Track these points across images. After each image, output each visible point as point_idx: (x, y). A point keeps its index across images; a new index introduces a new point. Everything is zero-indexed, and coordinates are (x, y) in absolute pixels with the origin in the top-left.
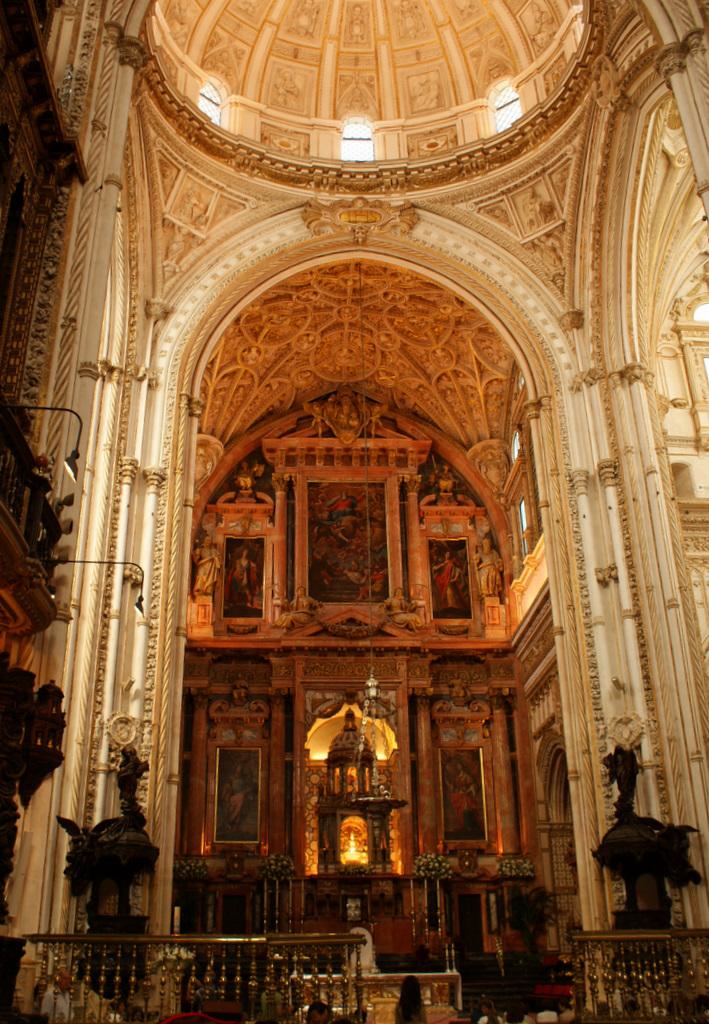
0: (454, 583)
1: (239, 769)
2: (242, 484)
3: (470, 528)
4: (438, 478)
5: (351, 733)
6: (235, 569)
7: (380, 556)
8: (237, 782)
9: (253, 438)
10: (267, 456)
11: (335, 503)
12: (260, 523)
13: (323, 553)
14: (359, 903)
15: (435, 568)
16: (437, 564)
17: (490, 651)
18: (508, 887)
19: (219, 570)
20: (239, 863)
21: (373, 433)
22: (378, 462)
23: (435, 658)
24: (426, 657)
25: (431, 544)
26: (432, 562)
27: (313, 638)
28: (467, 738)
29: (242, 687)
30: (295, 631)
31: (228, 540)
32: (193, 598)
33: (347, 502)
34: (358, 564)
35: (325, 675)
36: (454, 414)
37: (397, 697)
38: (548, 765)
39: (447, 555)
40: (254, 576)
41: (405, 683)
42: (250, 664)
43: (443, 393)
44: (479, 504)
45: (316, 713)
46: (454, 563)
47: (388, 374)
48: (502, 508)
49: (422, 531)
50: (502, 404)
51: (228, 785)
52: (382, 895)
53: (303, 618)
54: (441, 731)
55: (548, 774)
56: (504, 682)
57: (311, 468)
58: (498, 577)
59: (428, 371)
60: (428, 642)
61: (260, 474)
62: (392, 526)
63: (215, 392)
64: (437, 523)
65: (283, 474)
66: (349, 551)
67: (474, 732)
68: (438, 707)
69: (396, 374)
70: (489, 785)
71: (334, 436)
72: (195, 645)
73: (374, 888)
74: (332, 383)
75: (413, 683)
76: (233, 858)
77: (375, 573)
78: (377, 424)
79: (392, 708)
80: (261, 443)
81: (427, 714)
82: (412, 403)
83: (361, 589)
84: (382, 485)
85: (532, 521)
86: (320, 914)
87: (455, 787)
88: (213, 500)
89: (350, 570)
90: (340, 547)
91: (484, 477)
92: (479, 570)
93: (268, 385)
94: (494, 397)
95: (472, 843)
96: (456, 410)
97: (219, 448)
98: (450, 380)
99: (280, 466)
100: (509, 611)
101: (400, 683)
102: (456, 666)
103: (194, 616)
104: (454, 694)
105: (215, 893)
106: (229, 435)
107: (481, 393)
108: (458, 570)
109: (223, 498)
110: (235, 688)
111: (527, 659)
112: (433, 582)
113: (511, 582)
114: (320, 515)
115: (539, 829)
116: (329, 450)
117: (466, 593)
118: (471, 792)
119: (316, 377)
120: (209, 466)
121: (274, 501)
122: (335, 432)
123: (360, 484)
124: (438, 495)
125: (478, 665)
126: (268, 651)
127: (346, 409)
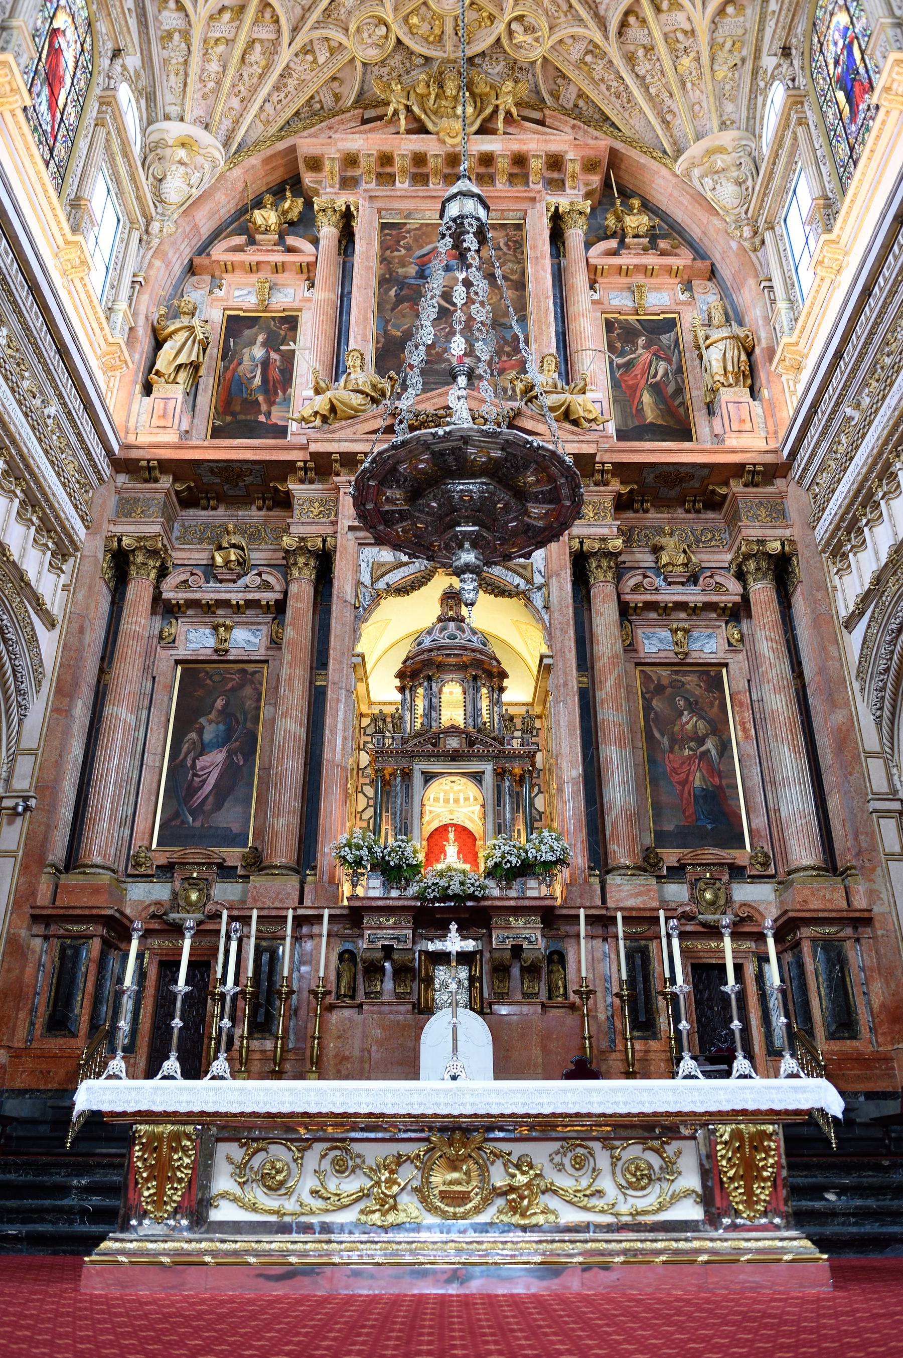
0: (656, 383)
1: (220, 703)
2: (259, 221)
3: (683, 297)
4: (619, 219)
5: (452, 625)
6: (240, 364)
9: (281, 146)
10: (308, 178)
12: (292, 291)
14: (463, 974)
15: (621, 361)
16: (622, 354)
17: (738, 470)
18: (814, 940)
19: (204, 346)
20: (200, 890)
21: (500, 125)
22: (510, 182)
23: (625, 490)
24: (606, 484)
25: (609, 326)
28: (696, 646)
29: (234, 546)
30: (337, 425)
31: (229, 316)
32: (148, 389)
36: (650, 98)
37: (546, 558)
38: (887, 670)
39: (641, 341)
40: (275, 374)
42: (254, 512)
43: (630, 59)
44: (699, 254)
45: (381, 585)
46: (654, 354)
47: (529, 29)
48: (746, 244)
49: (594, 302)
50: (743, 60)
51: (194, 735)
52: (517, 950)
53: (357, 400)
54: (639, 631)
55: (888, 694)
56: (769, 532)
58: (743, 357)
59: (602, 13)
61: (294, 215)
62: (537, 279)
63: (205, 42)
64: (621, 290)
65: (333, 201)
67: (709, 636)
68: (632, 582)
69: (545, 26)
70: (747, 737)
71: (427, 132)
72: (134, 454)
74: (428, 60)
77: (505, 358)
78: (508, 113)
79: (538, 579)
81: (610, 589)
82: (573, 96)
84: (519, 227)
85: (823, 188)
86: (366, 994)
87: (673, 741)
88: (204, 249)
91: (709, 195)
92: (707, 348)
93: (307, 50)
94: (728, 45)
95: (711, 853)
96: (653, 91)
97: (218, 156)
98: (644, 22)
99: (328, 190)
100: (771, 410)
102: (667, 516)
103: (145, 418)
104: (665, 559)
106: (238, 139)
107: (703, 38)
108: (662, 366)
110: (220, 548)
111: (822, 469)
112: (616, 384)
113: (771, 360)
114: (400, 270)
115: (876, 811)
116: (419, 159)
117: (680, 400)
118: (708, 751)
119: (399, 41)
120: (195, 178)
121: (317, 249)
122: (430, 126)
124: (622, 243)
125: (710, 515)
126: (287, 468)
127: (451, 88)
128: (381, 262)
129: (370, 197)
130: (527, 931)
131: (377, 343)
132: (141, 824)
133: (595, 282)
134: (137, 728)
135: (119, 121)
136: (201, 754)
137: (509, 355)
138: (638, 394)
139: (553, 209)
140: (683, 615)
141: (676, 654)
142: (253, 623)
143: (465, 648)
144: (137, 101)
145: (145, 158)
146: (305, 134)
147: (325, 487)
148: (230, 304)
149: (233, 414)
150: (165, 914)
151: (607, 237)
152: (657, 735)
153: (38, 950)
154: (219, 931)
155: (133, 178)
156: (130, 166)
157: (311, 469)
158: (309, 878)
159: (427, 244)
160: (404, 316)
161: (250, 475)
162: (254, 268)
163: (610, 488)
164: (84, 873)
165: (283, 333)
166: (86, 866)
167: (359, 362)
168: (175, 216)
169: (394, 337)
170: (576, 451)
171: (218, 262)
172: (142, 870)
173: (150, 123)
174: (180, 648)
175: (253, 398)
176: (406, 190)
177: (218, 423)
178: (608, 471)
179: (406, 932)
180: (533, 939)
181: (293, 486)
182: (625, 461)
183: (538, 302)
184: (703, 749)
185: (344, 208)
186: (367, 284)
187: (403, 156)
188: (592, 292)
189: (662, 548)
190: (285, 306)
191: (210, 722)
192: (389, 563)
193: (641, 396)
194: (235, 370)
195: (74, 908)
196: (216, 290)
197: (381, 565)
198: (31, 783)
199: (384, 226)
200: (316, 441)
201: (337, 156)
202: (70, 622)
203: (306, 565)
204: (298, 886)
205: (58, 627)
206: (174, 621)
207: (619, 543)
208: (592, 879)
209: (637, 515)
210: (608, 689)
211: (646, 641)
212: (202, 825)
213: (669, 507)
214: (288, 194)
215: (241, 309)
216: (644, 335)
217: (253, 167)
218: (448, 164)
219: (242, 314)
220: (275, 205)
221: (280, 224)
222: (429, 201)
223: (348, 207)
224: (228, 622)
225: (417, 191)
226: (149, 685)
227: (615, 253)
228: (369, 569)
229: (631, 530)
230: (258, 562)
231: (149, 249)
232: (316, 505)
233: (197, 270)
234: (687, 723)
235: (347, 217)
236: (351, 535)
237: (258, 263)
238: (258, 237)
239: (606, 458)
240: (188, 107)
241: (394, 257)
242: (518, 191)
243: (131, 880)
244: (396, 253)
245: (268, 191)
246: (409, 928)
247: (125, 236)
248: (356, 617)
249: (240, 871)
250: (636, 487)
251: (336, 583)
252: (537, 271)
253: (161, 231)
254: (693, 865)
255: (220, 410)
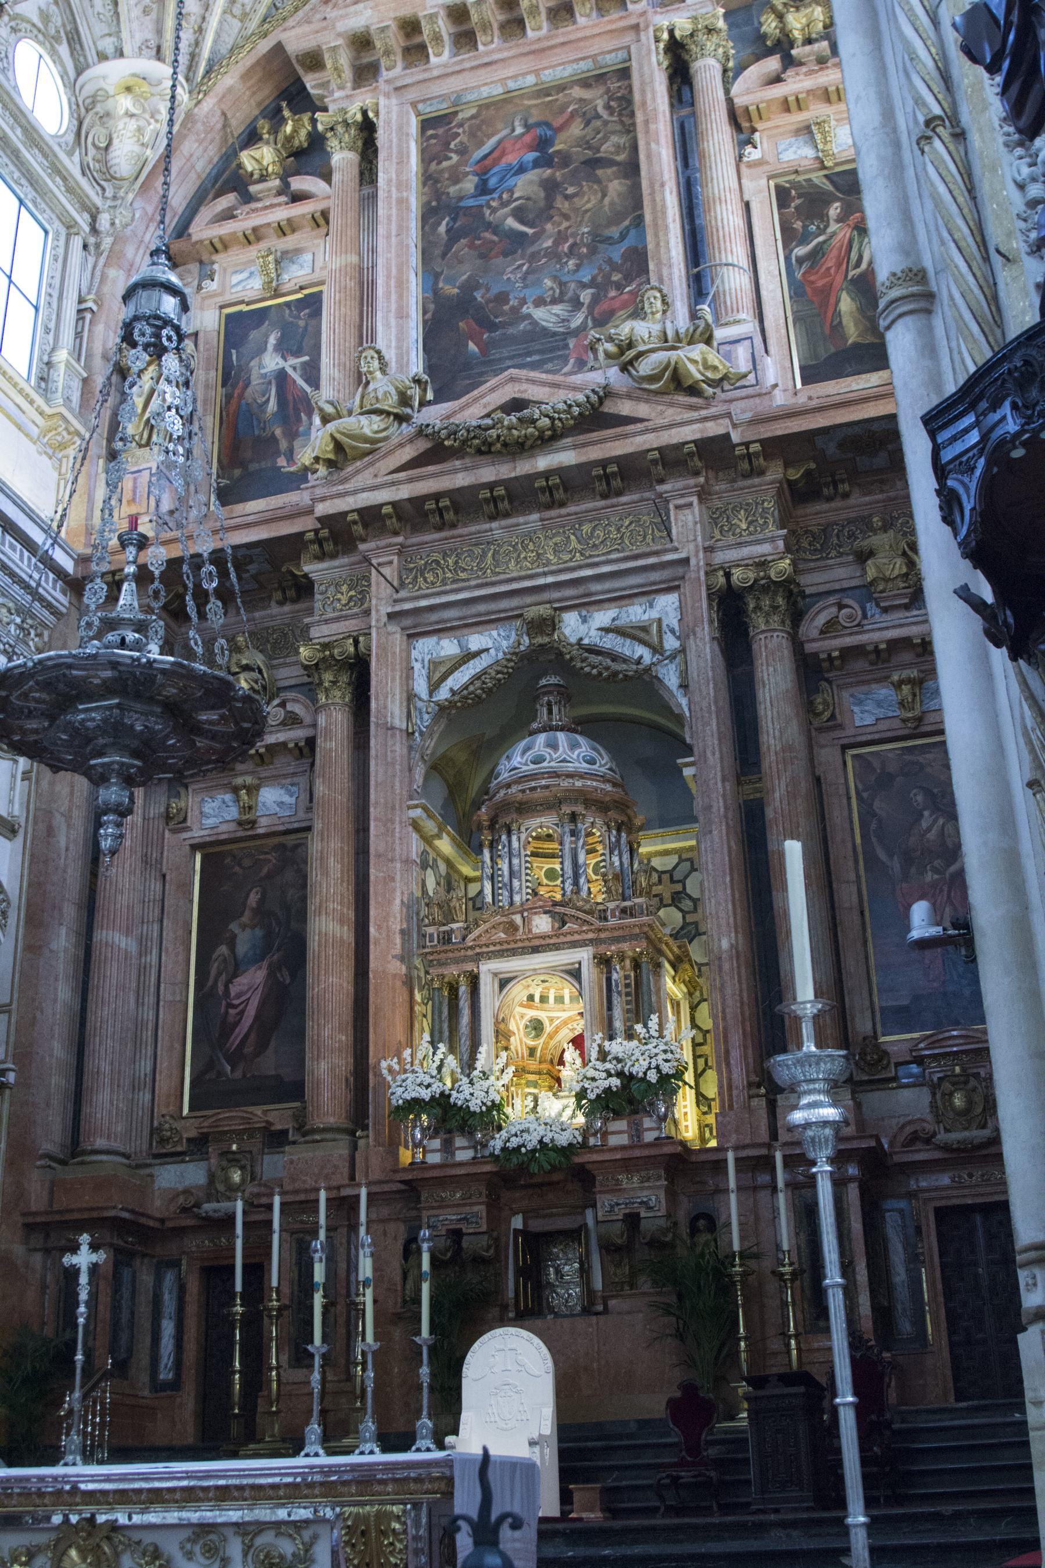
1: (253, 899)
2: (249, 165)
4: (780, 17)
6: (247, 384)
7: (623, 247)
8: (245, 940)
9: (265, 46)
10: (311, 82)
11: (499, 143)
13: (464, 277)
15: (801, 251)
16: (804, 240)
20: (242, 1168)
22: (599, 9)
23: (794, 474)
24: (761, 473)
25: (783, 196)
26: (789, 236)
27: (402, 475)
29: (247, 668)
30: (350, 469)
31: (228, 317)
33: (528, 138)
34: (562, 285)
35: (454, 581)
39: (834, 210)
41: (698, 562)
42: (275, 610)
51: (223, 949)
52: (632, 1220)
53: (370, 426)
57: (416, 74)
60: (757, 421)
62: (649, 156)
66: (534, 257)
68: (821, 620)
73: (604, 1201)
75: (721, 557)
76: (226, 1154)
77: (613, 293)
79: (671, 643)
80: (288, 57)
83: (572, 343)
84: (624, 73)
87: (908, 860)
89: (540, 302)
90: (505, 254)
99: (337, 94)
101: (686, 561)
105: (176, 1264)
106: (206, 53)
109: (206, 214)
112: (797, 291)
114: (452, 190)
123: (562, 88)
126: (294, 545)
128: (424, 184)
129: (397, 89)
130: (645, 1193)
131: (425, 312)
132: (164, 1084)
133: (754, 130)
134: (143, 951)
135: (11, 106)
136: (235, 975)
137: (619, 287)
138: (832, 300)
139: (665, 36)
140: (907, 657)
141: (904, 721)
142: (285, 776)
143: (555, 774)
144: (54, 54)
145: (80, 124)
146: (291, 22)
147: (353, 559)
148: (228, 297)
149: (243, 464)
150: (198, 1205)
151: (769, 52)
152: (883, 856)
153: (38, 1266)
154: (270, 1222)
155: (57, 170)
156: (45, 156)
157: (326, 539)
158: (361, 1143)
159: (489, 136)
160: (460, 262)
161: (251, 562)
162: (252, 238)
163: (769, 477)
164: (83, 1163)
165: (302, 323)
166: (84, 1153)
167: (376, 364)
168: (130, 196)
169: (449, 298)
170: (698, 436)
171: (201, 242)
172: (169, 1148)
173: (79, 72)
174: (195, 827)
175: (267, 433)
176: (445, 66)
177: (224, 482)
178: (756, 454)
179: (476, 1209)
180: (652, 1204)
181: (310, 568)
182: (779, 433)
183: (652, 193)
184: (953, 869)
185: (359, 117)
186: (400, 228)
187: (432, 17)
188: (749, 149)
189: (871, 554)
190: (302, 282)
191: (244, 927)
192: (449, 658)
193: (838, 301)
194: (241, 396)
195: (72, 1211)
196: (206, 283)
197: (434, 664)
198: (7, 1051)
199: (427, 124)
200: (323, 499)
201: (340, 42)
202: (35, 823)
203: (334, 683)
204: (345, 1152)
205: (21, 831)
206: (182, 791)
207: (785, 564)
208: (755, 1102)
209: (833, 505)
210: (778, 804)
211: (856, 709)
212: (244, 1076)
213: (882, 482)
214: (286, 113)
215: (242, 302)
216: (838, 199)
217: (230, 90)
218: (501, 8)
219: (244, 308)
220: (275, 130)
221: (281, 162)
222: (482, 71)
223: (364, 113)
224: (249, 780)
225: (463, 60)
226: (159, 886)
227: (777, 79)
228: (424, 672)
229: (825, 530)
230: (286, 683)
231: (99, 255)
232: (344, 588)
233: (178, 260)
234: (929, 829)
235: (367, 128)
236: (393, 628)
237: (255, 230)
238: (253, 189)
239: (750, 436)
240: (125, 35)
241: (442, 171)
242: (611, 22)
243: (158, 1161)
244: (445, 164)
245: (264, 114)
246: (480, 1203)
247: (61, 251)
248: (410, 748)
249: (291, 1138)
250: (813, 466)
251: (373, 705)
252: (648, 144)
253: (113, 224)
254: (934, 1057)
255: (225, 462)
